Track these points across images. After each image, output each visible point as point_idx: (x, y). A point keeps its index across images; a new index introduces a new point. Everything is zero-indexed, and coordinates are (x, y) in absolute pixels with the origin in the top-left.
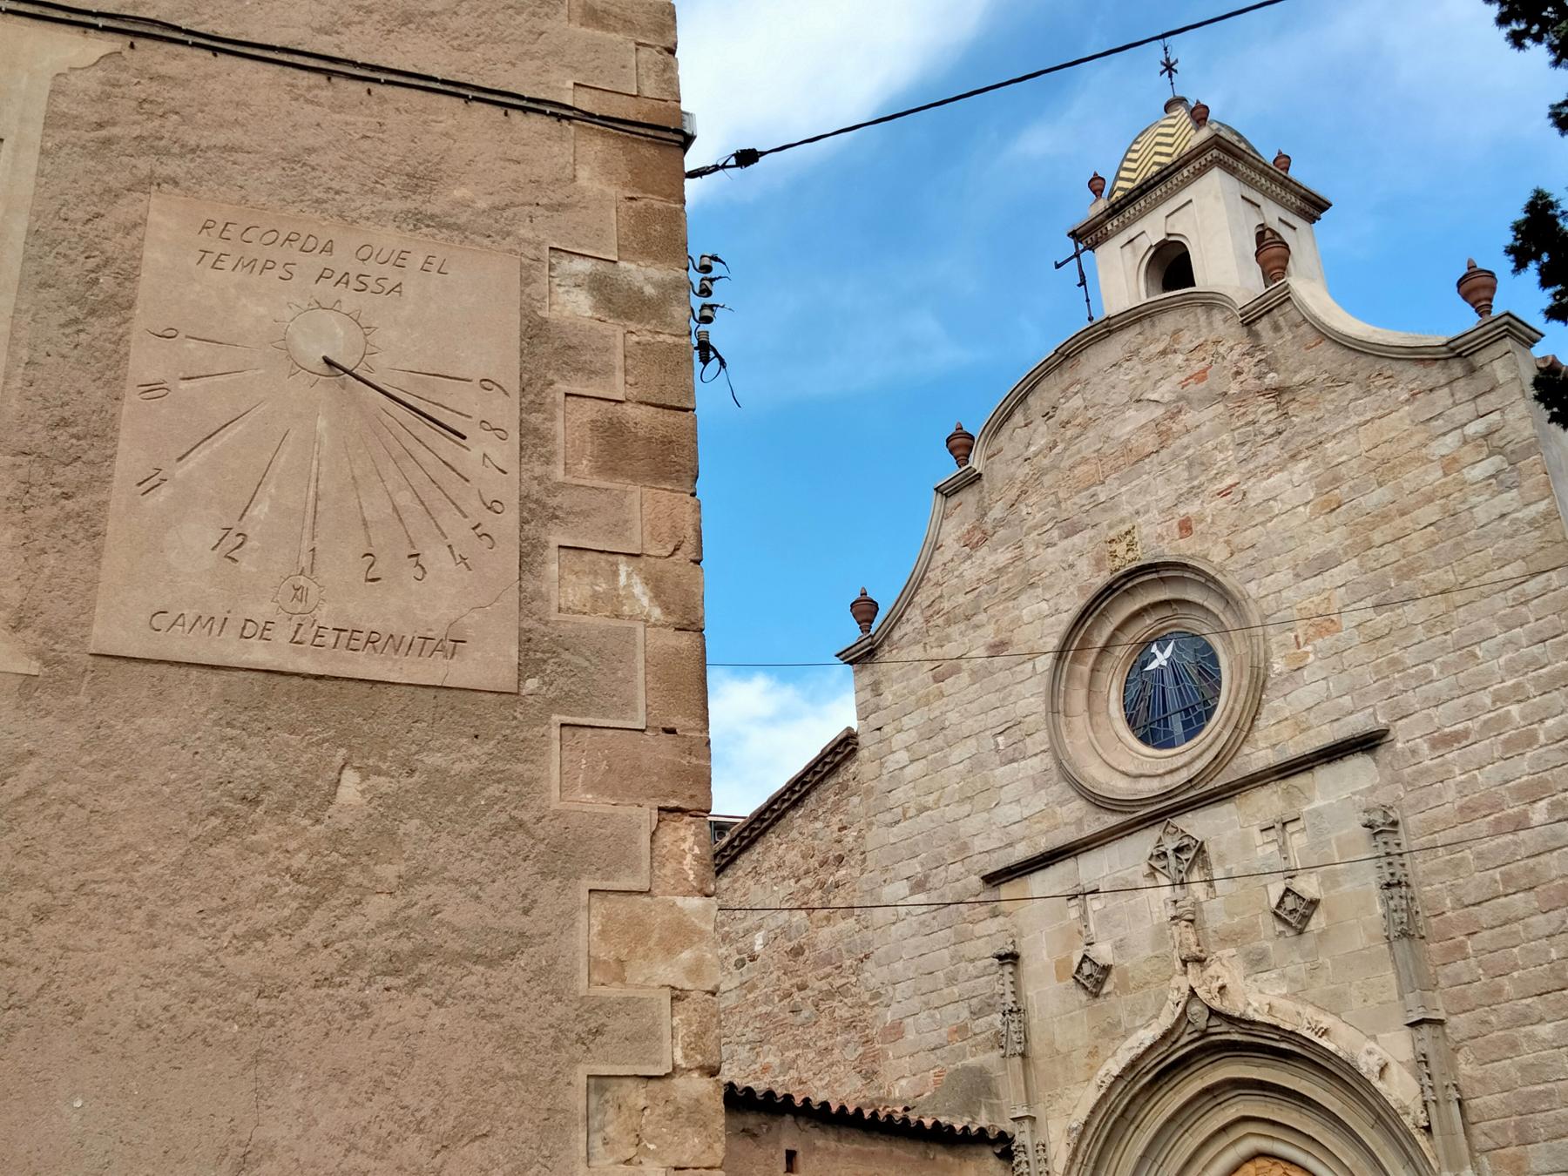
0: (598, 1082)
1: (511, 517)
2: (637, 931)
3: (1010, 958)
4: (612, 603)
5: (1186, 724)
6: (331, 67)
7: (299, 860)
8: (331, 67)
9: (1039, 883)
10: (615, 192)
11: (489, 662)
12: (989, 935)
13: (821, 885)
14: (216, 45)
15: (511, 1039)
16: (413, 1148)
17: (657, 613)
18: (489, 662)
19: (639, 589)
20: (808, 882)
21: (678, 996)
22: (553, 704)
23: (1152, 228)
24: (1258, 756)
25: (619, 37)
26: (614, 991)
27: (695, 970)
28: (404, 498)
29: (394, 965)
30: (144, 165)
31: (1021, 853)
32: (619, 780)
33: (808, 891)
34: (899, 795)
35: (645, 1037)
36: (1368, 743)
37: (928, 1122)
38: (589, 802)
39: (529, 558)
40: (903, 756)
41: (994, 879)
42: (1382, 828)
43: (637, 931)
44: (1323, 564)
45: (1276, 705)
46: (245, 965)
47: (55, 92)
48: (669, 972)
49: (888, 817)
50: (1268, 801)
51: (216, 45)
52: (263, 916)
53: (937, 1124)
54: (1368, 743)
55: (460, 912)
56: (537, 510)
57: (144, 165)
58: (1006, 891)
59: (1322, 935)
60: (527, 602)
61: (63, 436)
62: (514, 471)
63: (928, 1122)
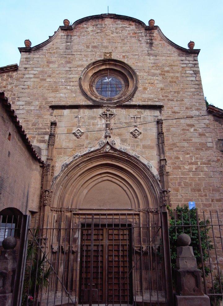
9: (66, 112)
36: (159, 108)
41: (53, 107)
45: (137, 94)
50: (134, 112)
54: (159, 108)
58: (56, 112)
59: (141, 140)
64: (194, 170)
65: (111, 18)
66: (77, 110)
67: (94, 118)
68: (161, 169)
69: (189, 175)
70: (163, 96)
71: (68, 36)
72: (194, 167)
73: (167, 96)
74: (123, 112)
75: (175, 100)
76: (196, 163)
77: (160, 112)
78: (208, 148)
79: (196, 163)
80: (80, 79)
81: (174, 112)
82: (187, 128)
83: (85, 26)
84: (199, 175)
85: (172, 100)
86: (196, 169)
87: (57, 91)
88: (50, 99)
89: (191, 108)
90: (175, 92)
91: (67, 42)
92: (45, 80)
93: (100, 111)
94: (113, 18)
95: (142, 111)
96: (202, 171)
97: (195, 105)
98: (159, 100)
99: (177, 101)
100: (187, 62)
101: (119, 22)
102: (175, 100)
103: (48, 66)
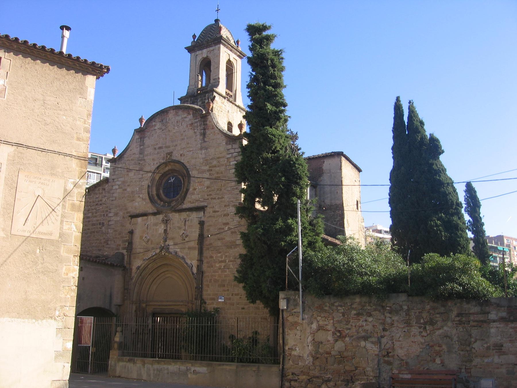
0: (63, 287)
1: (60, 217)
3: (131, 233)
5: (174, 195)
6: (43, 150)
7: (33, 260)
8: (43, 150)
9: (140, 219)
10: (77, 169)
11: (55, 237)
12: (129, 227)
13: (95, 209)
14: (28, 147)
17: (76, 230)
18: (55, 237)
19: (74, 227)
20: (93, 208)
23: (204, 53)
24: (185, 206)
25: (81, 143)
26: (66, 277)
29: (42, 272)
30: (18, 166)
31: (138, 212)
33: (92, 210)
34: (115, 195)
36: (202, 209)
37: (109, 263)
39: (62, 222)
40: (117, 187)
42: (202, 224)
44: (203, 172)
46: (26, 271)
47: (8, 156)
49: (111, 199)
50: (184, 215)
51: (28, 147)
52: (28, 266)
53: (111, 264)
54: (202, 209)
56: (63, 216)
57: (18, 166)
58: (134, 220)
60: (61, 228)
61: (8, 206)
62: (61, 211)
63: (109, 263)
64: (222, 267)
65: (174, 109)
66: (146, 217)
67: (156, 224)
68: (199, 267)
69: (218, 272)
70: (208, 195)
71: (141, 138)
72: (223, 264)
73: (211, 195)
74: (176, 215)
75: (217, 198)
76: (225, 261)
77: (204, 213)
78: (237, 246)
79: (225, 261)
80: (149, 186)
81: (215, 212)
82: (223, 227)
83: (154, 124)
84: (225, 272)
85: (215, 199)
86: (224, 267)
87: (133, 200)
88: (130, 209)
89: (229, 205)
90: (218, 189)
91: (140, 146)
92: (126, 190)
93: (161, 217)
94: (175, 109)
95: (190, 213)
96: (228, 269)
97: (232, 201)
98: (204, 199)
99: (218, 198)
100: (232, 151)
101: (180, 112)
102: (217, 198)
103: (128, 175)
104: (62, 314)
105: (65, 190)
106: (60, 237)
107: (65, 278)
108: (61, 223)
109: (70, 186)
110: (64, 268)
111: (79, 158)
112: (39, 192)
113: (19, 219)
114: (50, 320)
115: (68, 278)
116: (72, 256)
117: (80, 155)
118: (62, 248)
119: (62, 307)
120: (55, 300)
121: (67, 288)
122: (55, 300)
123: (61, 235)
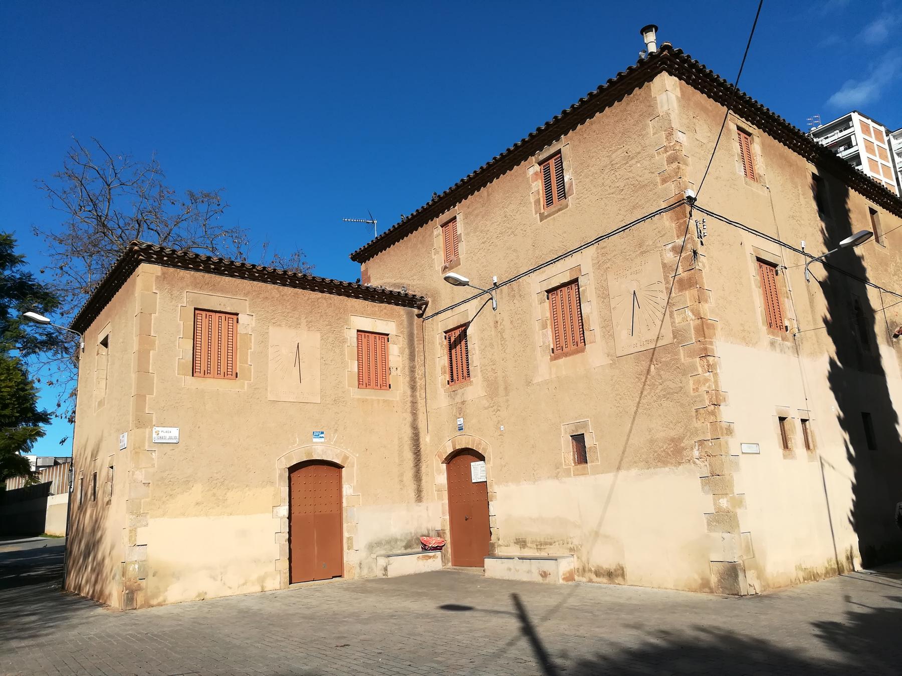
0: (697, 410)
2: (698, 382)
4: (685, 319)
14: (608, 236)
15: (682, 405)
16: (671, 425)
19: (690, 314)
21: (708, 392)
22: (679, 343)
26: (697, 394)
27: (709, 387)
28: (650, 312)
32: (691, 354)
35: (702, 401)
38: (689, 360)
43: (698, 382)
48: (705, 388)
51: (608, 236)
55: (672, 385)
60: (673, 323)
104: (703, 454)
105: (664, 266)
106: (675, 337)
107: (695, 397)
108: (671, 317)
109: (670, 257)
110: (691, 382)
111: (670, 208)
112: (634, 287)
113: (623, 334)
114: (687, 466)
115: (699, 396)
116: (698, 359)
117: (672, 201)
118: (682, 352)
119: (701, 443)
120: (688, 434)
121: (702, 411)
122: (688, 434)
123: (675, 334)
